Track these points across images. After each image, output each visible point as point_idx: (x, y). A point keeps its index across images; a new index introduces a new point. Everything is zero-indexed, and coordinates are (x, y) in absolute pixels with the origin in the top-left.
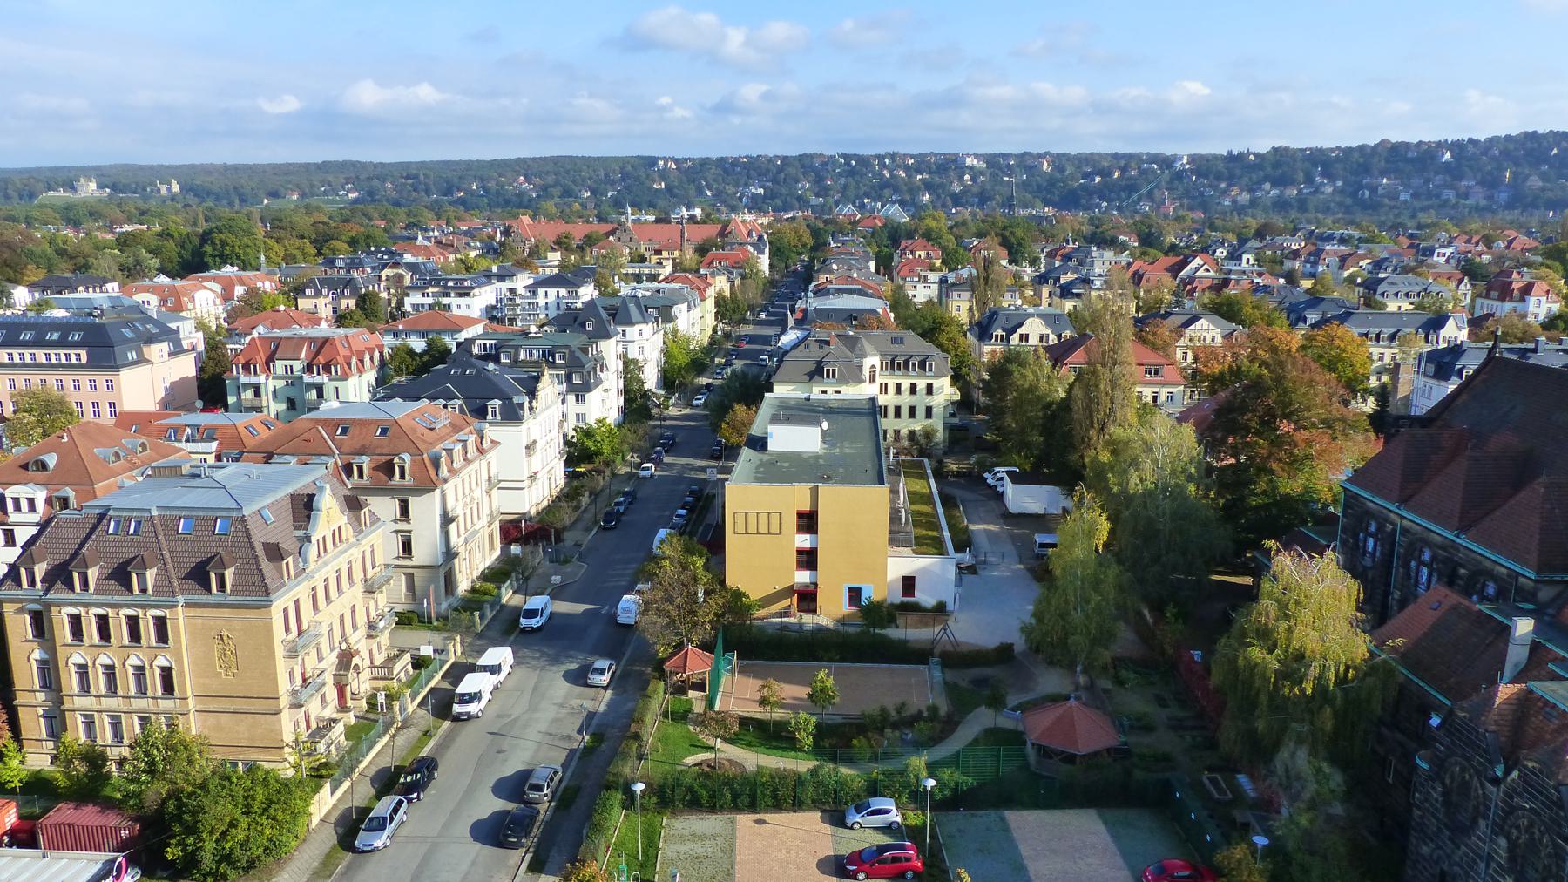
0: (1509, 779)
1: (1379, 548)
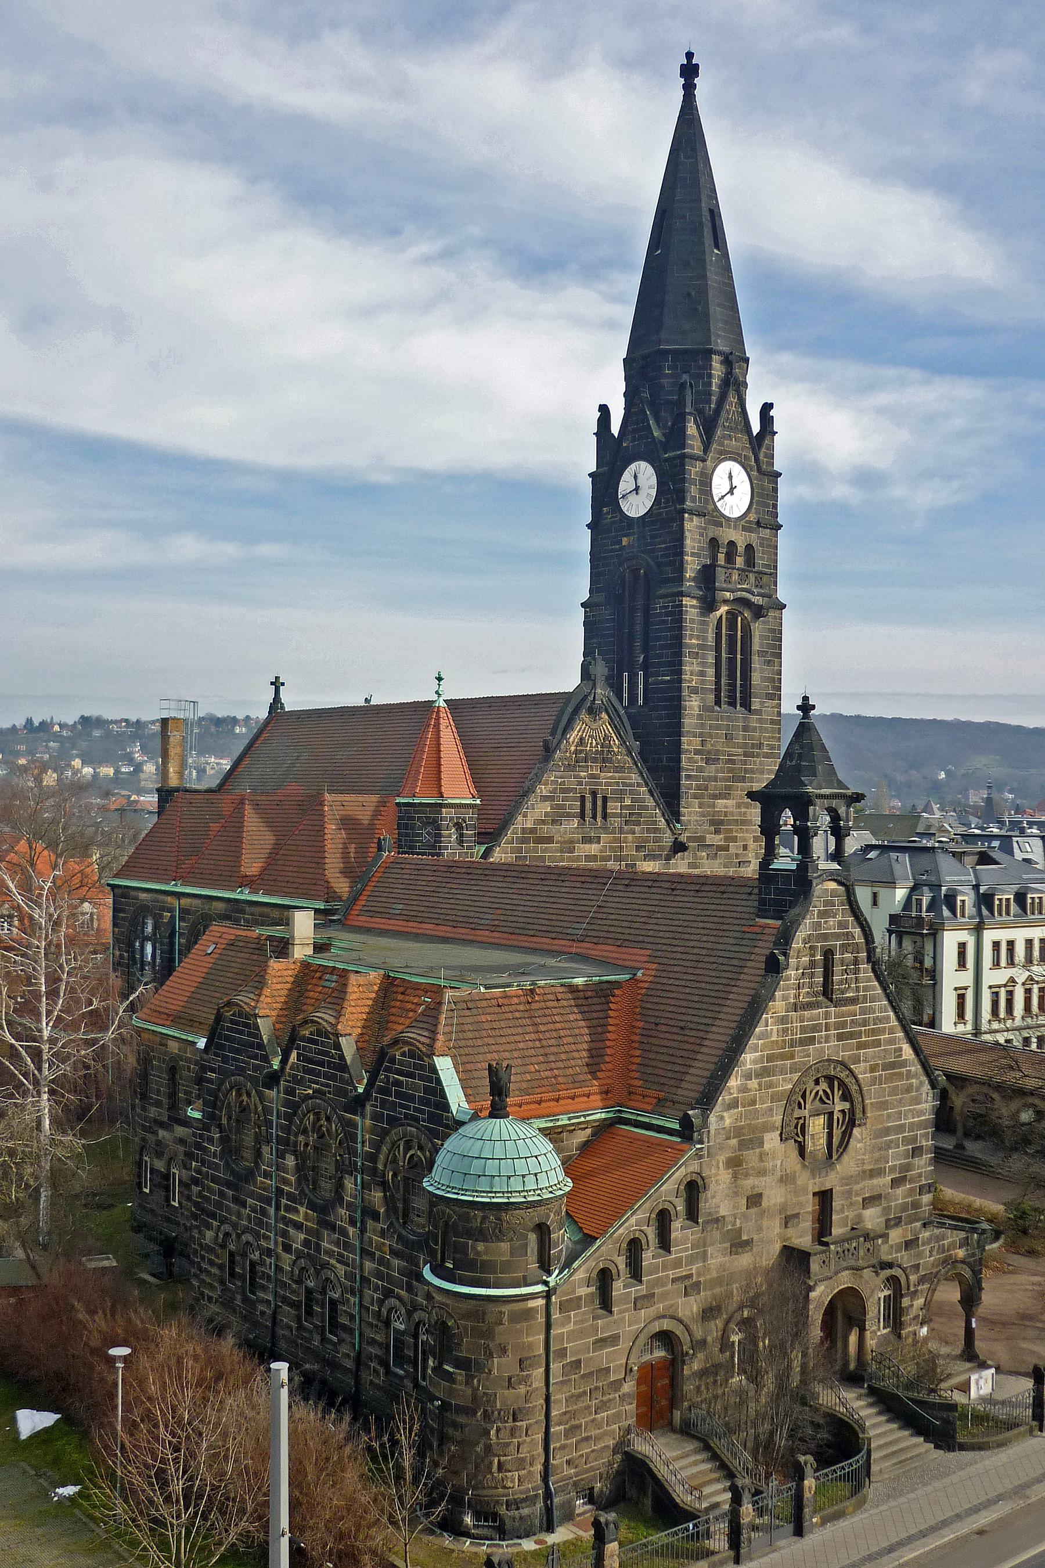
0: (288, 1067)
1: (158, 952)
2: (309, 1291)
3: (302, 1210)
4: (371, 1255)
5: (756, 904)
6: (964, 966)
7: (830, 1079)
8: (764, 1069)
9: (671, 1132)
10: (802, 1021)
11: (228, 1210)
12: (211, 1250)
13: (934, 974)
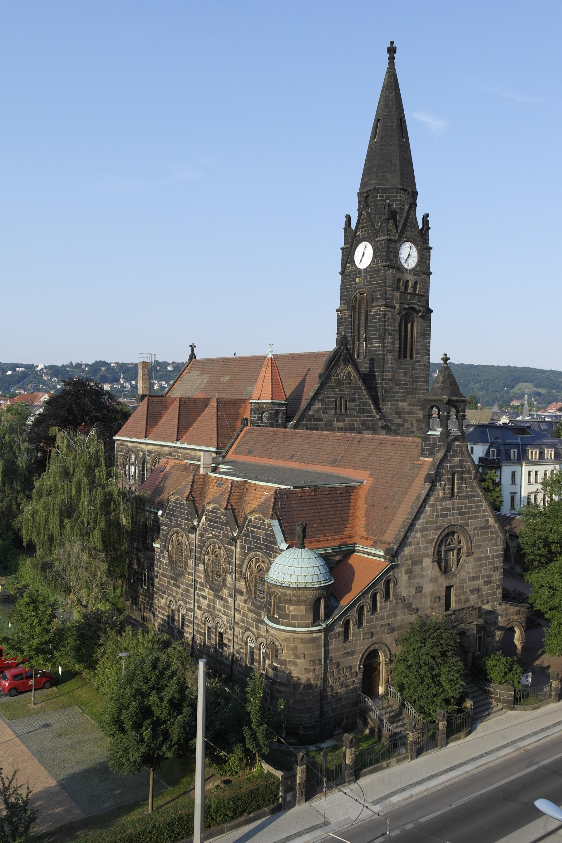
0: (201, 524)
2: (209, 628)
3: (207, 590)
4: (239, 611)
8: (423, 528)
11: (172, 590)
12: (164, 609)
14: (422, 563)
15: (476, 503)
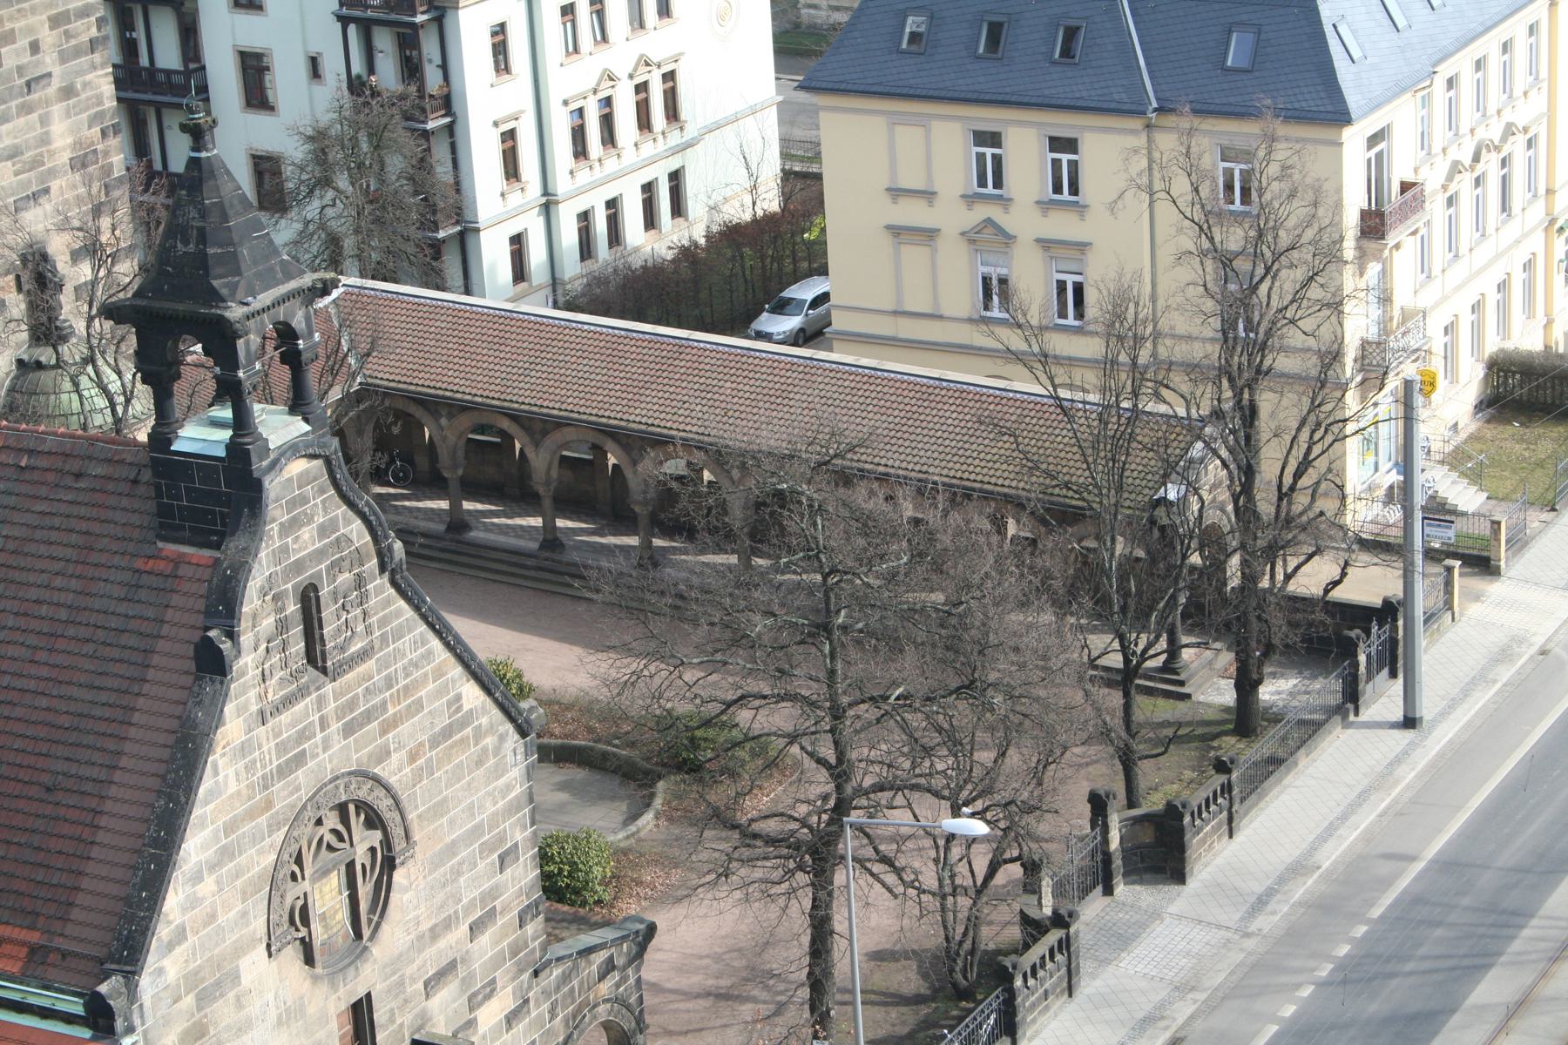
5: (151, 506)
6: (507, 70)
7: (342, 809)
9: (69, 1019)
10: (276, 735)
13: (447, 103)
14: (235, 978)
15: (404, 655)
